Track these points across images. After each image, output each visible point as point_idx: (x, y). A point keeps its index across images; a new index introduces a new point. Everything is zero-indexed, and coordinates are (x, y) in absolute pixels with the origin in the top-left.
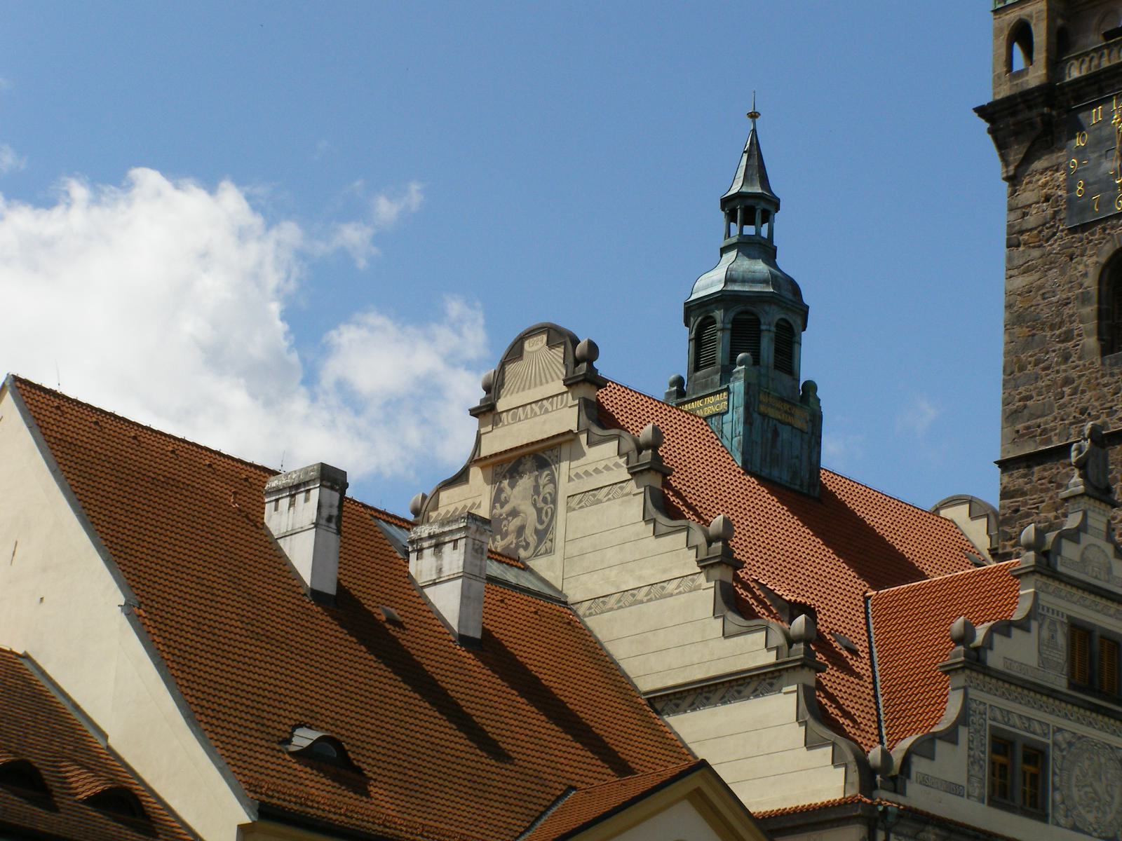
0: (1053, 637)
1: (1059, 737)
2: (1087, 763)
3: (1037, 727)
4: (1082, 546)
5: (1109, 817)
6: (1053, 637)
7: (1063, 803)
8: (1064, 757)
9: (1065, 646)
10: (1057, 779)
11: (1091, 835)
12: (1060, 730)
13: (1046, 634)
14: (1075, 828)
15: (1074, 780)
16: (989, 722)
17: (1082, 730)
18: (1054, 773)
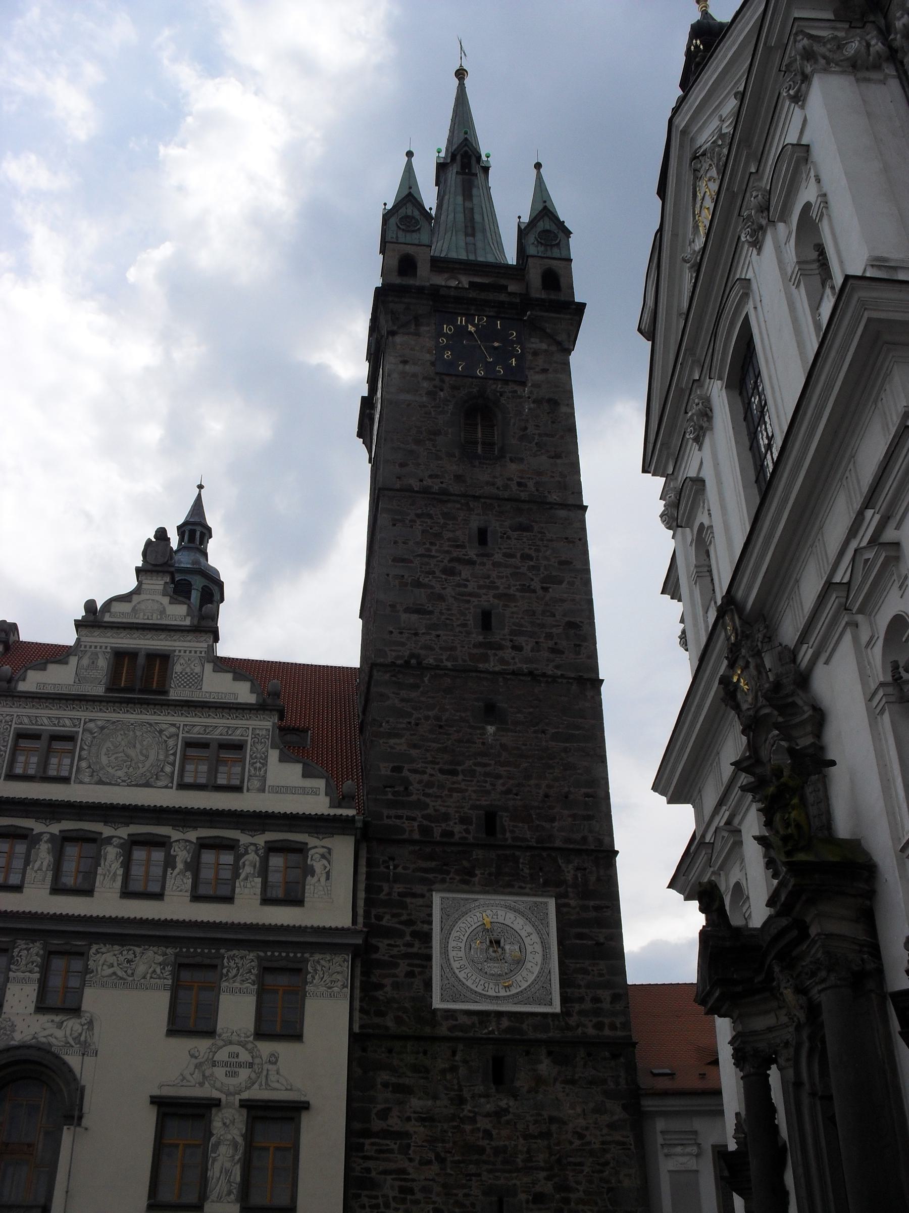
0: (93, 663)
1: (91, 725)
2: (119, 738)
3: (67, 722)
4: (134, 603)
5: (142, 770)
6: (93, 663)
7: (89, 767)
8: (94, 737)
9: (105, 666)
10: (84, 753)
11: (119, 785)
12: (91, 720)
13: (85, 661)
14: (100, 782)
15: (104, 750)
16: (14, 726)
17: (114, 716)
18: (82, 749)
